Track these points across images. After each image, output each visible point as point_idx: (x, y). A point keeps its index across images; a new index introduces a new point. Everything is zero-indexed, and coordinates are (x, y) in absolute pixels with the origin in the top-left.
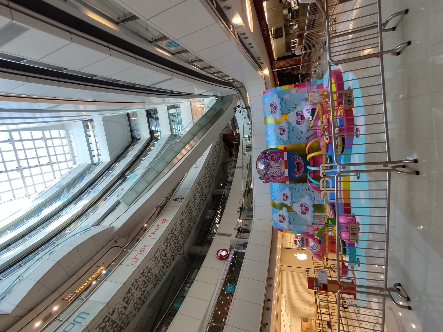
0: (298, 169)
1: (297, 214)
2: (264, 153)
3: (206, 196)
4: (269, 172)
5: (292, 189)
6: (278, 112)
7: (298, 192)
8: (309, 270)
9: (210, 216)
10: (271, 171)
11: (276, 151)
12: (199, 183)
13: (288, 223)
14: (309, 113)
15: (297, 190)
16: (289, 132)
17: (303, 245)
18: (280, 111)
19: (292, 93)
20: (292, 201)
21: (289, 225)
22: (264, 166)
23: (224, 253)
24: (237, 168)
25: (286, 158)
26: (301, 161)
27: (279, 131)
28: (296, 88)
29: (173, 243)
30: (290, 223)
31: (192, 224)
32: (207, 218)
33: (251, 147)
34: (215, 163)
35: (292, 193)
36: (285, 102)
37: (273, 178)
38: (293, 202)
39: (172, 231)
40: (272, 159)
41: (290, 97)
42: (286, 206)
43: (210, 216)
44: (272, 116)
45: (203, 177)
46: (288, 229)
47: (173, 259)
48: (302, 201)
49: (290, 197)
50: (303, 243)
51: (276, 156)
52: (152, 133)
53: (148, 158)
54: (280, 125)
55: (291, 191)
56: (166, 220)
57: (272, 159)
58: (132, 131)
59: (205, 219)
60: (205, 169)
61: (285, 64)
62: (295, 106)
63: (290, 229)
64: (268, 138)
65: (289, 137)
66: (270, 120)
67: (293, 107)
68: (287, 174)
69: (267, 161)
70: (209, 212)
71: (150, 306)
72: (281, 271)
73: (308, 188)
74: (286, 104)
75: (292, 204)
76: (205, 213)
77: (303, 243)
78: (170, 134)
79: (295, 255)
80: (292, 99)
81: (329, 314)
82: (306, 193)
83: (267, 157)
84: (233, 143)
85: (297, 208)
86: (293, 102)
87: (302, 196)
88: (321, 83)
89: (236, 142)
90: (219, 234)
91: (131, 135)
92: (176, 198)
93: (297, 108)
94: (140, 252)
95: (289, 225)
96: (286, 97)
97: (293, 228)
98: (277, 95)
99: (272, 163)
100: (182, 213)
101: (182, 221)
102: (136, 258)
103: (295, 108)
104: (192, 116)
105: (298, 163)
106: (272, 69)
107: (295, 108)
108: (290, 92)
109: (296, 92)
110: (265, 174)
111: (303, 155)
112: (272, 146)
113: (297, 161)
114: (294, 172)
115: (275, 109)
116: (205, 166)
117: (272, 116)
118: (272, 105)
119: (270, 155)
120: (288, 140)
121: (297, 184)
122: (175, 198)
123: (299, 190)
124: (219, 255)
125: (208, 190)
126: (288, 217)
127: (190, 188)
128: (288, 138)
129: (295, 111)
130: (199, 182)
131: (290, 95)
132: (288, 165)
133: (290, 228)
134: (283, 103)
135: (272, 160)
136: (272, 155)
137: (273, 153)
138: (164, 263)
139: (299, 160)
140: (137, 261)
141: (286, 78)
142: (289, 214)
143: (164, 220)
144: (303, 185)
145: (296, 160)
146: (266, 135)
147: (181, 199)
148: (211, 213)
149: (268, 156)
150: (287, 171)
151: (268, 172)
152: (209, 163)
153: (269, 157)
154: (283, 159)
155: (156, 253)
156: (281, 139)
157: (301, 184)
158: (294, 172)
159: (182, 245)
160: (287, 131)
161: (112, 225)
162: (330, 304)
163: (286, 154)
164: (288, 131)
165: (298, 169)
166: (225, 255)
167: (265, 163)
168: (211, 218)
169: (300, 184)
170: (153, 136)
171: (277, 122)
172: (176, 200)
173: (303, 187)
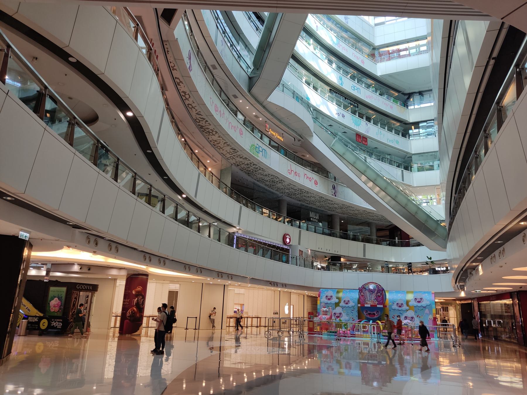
0: (369, 314)
1: (334, 309)
2: (383, 290)
3: (334, 210)
4: (367, 292)
5: (353, 308)
6: (416, 304)
7: (351, 312)
8: (278, 315)
9: (313, 218)
10: (368, 294)
11: (384, 300)
12: (350, 206)
13: (326, 302)
14: (406, 323)
15: (353, 312)
16: (399, 310)
17: (324, 312)
18: (416, 306)
19: (429, 315)
20: (343, 307)
21: (325, 303)
22: (372, 288)
23: (288, 240)
24: (364, 244)
25: (378, 306)
26: (376, 317)
27: (400, 303)
28: (432, 318)
29: (296, 192)
30: (326, 304)
31: (307, 202)
32: (312, 215)
33: (388, 273)
34: (371, 218)
35: (350, 307)
36: (422, 309)
37: (363, 295)
38: (343, 308)
39: (308, 192)
40: (378, 296)
41: (426, 313)
42: (339, 302)
43: (313, 218)
44: (413, 298)
45: (355, 209)
46: (322, 302)
47: (282, 193)
48: (344, 315)
49: (347, 305)
50: (325, 312)
51: (380, 299)
52: (416, 125)
53: (379, 133)
54: (405, 304)
55: (351, 307)
56: (317, 184)
57: (378, 296)
58: (421, 93)
59: (310, 212)
60: (365, 211)
61: (476, 312)
62: (419, 316)
63: (321, 303)
64: (395, 293)
65: (395, 310)
66: (410, 297)
67: (418, 315)
68: (366, 305)
69: (376, 291)
70: (316, 216)
71: (254, 183)
72: (272, 290)
73: (354, 320)
74: (421, 310)
75: (341, 307)
76: (316, 211)
77: (325, 312)
78: (413, 153)
79: (287, 304)
80: (425, 315)
81: (247, 326)
82: (350, 318)
83: (379, 292)
84: (397, 238)
85: (338, 310)
86: (422, 316)
87: (347, 315)
88: (435, 337)
89: (397, 242)
90: (300, 232)
91: (415, 93)
92: (336, 187)
93: (417, 318)
94: (295, 172)
95: (325, 303)
96: (427, 311)
97: (322, 305)
98: (429, 304)
99: (374, 295)
100: (321, 197)
101: (313, 197)
102: (291, 171)
103: (417, 317)
104: (437, 185)
105: (374, 314)
106: (473, 298)
107: (417, 317)
108: (430, 314)
109: (430, 318)
110: (365, 288)
111: (381, 319)
112: (388, 296)
113: (376, 314)
114: (367, 311)
115: (418, 301)
116: (367, 211)
117: (413, 298)
118: (422, 300)
119: (381, 295)
120: (393, 309)
121: (357, 312)
122: (335, 186)
123: (353, 313)
124: (287, 236)
125: (339, 212)
126: (331, 303)
127: (345, 200)
128: (394, 309)
129: (415, 316)
130: (350, 207)
131: (428, 313)
132: (373, 307)
133: (322, 304)
134: (422, 308)
135: (377, 296)
136: (381, 296)
137: (383, 297)
138: (282, 189)
139: (377, 316)
140: (290, 174)
141: (469, 311)
142: (334, 304)
143: (317, 183)
144: (357, 316)
145: (377, 313)
146: (397, 292)
147: (334, 193)
148: (315, 218)
149: (380, 293)
150: (369, 306)
151: (367, 291)
152: (371, 213)
153: (379, 294)
154: (378, 304)
155: (294, 185)
156: (394, 303)
157: (358, 315)
158: (367, 311)
159: (291, 197)
160: (400, 309)
161: (314, 134)
162: (267, 327)
163: (382, 306)
164: (400, 310)
165: (369, 314)
166: (287, 242)
167: (374, 289)
168: (311, 219)
169: (357, 314)
170: (412, 124)
171: (407, 302)
172: (334, 188)
173: (355, 316)
